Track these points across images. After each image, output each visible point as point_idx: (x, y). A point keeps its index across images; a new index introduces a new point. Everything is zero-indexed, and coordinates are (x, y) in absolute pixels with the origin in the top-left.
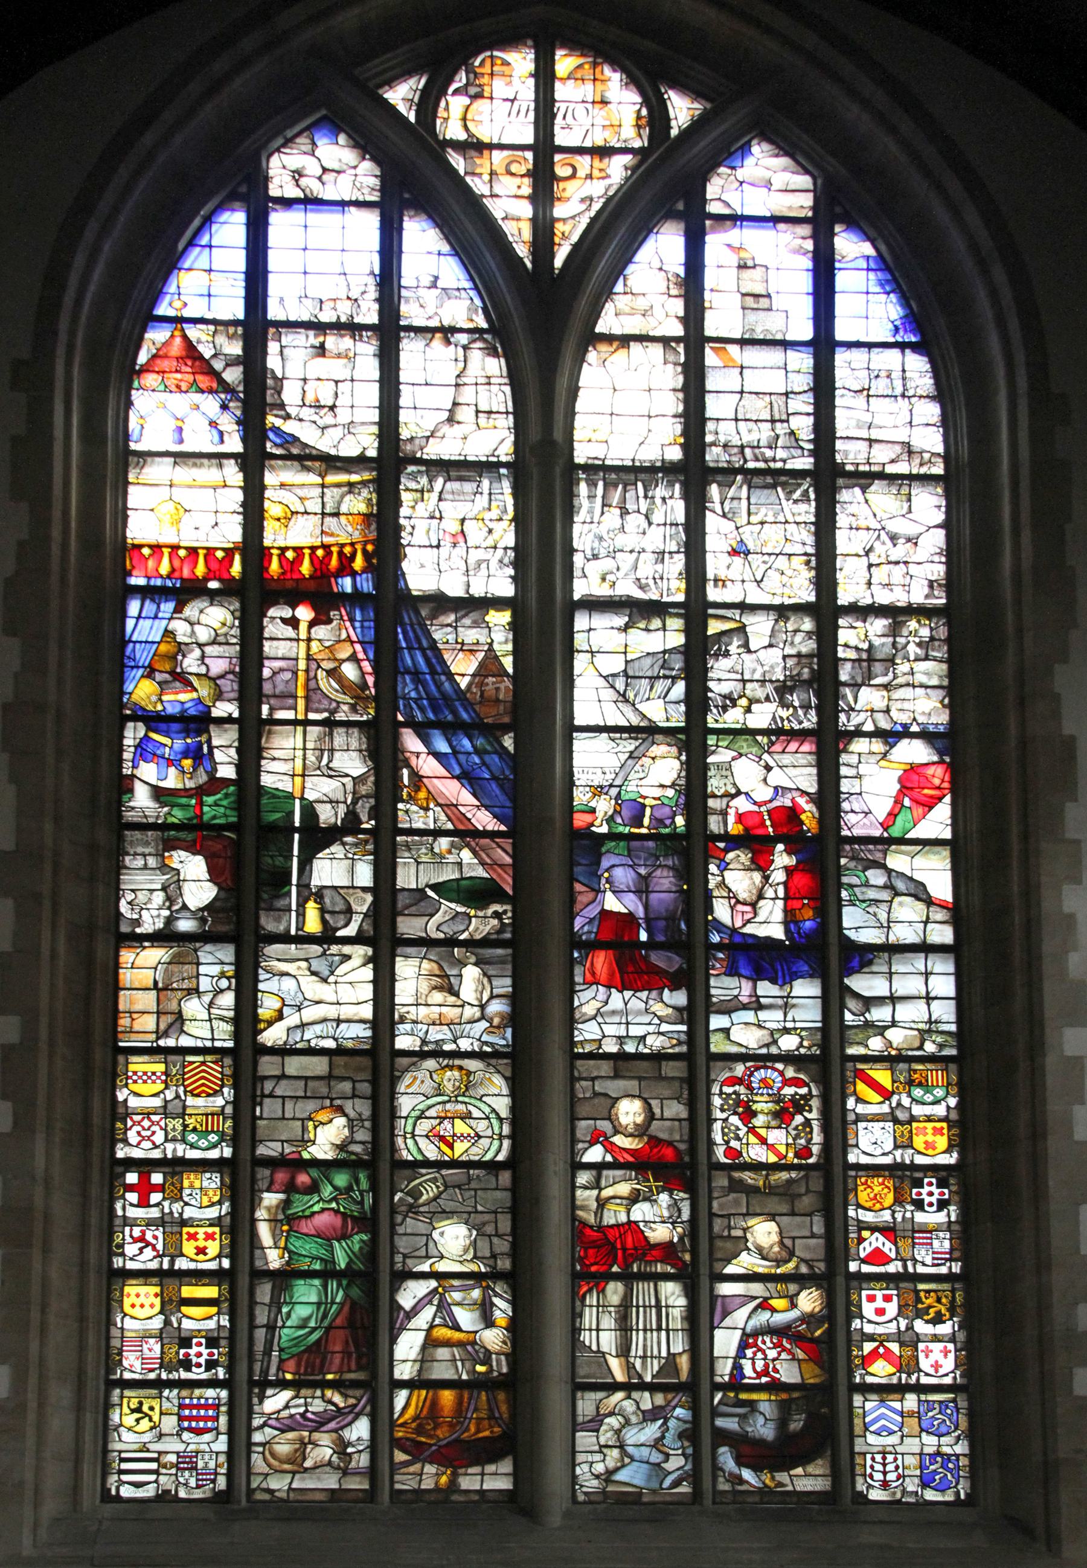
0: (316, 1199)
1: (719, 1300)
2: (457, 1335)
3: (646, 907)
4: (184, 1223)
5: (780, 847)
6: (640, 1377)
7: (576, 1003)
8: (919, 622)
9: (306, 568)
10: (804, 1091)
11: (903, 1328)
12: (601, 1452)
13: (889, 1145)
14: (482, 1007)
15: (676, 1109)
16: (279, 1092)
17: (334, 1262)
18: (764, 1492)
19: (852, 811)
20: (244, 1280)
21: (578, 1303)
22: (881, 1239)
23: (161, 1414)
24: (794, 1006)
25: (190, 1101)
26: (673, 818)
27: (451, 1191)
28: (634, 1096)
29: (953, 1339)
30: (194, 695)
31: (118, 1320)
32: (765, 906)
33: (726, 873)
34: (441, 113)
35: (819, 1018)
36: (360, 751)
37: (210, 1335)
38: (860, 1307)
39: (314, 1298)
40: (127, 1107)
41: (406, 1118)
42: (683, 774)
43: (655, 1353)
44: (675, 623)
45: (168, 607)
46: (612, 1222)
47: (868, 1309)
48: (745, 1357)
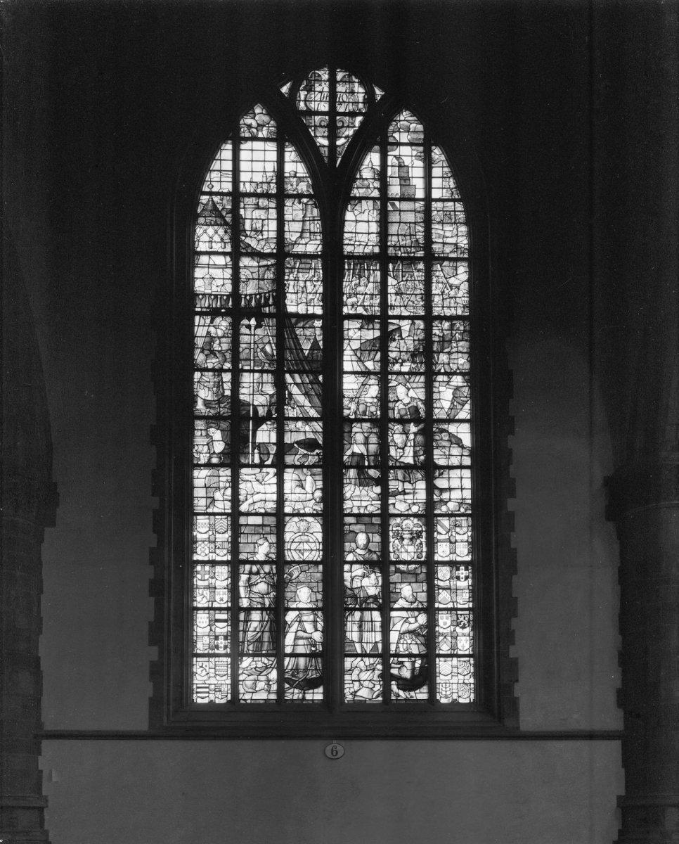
10: (420, 529)
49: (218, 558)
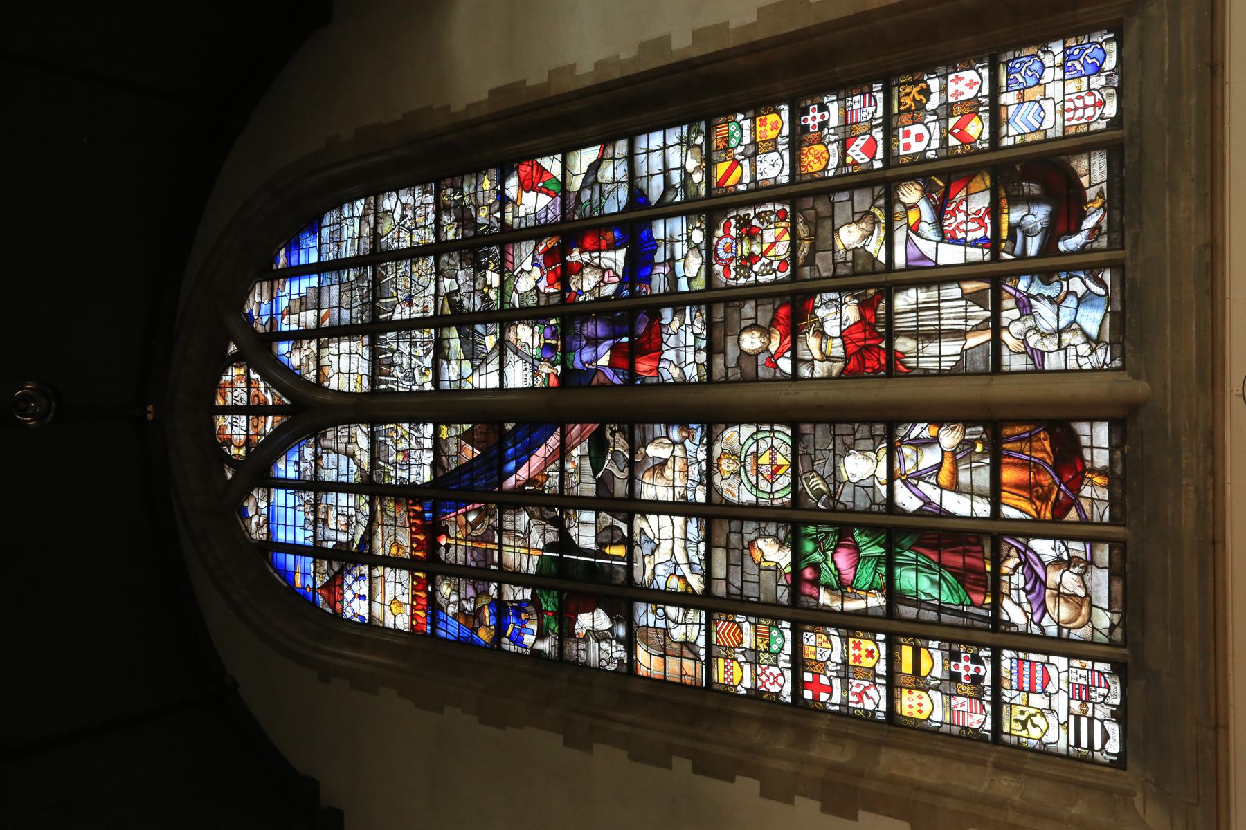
0: (824, 565)
1: (909, 263)
2: (947, 466)
3: (606, 339)
4: (845, 663)
5: (568, 258)
6: (986, 320)
7: (672, 381)
8: (443, 196)
9: (421, 537)
10: (733, 222)
11: (935, 117)
12: (1066, 349)
13: (775, 155)
14: (674, 443)
15: (749, 309)
16: (738, 584)
17: (879, 557)
18: (1108, 208)
19: (546, 217)
20: (895, 626)
21: (915, 372)
22: (853, 147)
23: (1027, 705)
24: (671, 236)
25: (746, 645)
26: (551, 326)
27: (816, 468)
28: (739, 339)
29: (946, 77)
30: (486, 607)
31: (933, 724)
32: (606, 263)
33: (585, 290)
34: (236, 458)
35: (680, 218)
36: (515, 514)
37: (947, 657)
38: (915, 154)
39: (913, 574)
40: (751, 689)
41: (757, 498)
42: (526, 322)
43: (962, 309)
44: (445, 332)
45: (442, 616)
46: (841, 349)
47: (917, 147)
48: (965, 239)
49: (788, 648)
